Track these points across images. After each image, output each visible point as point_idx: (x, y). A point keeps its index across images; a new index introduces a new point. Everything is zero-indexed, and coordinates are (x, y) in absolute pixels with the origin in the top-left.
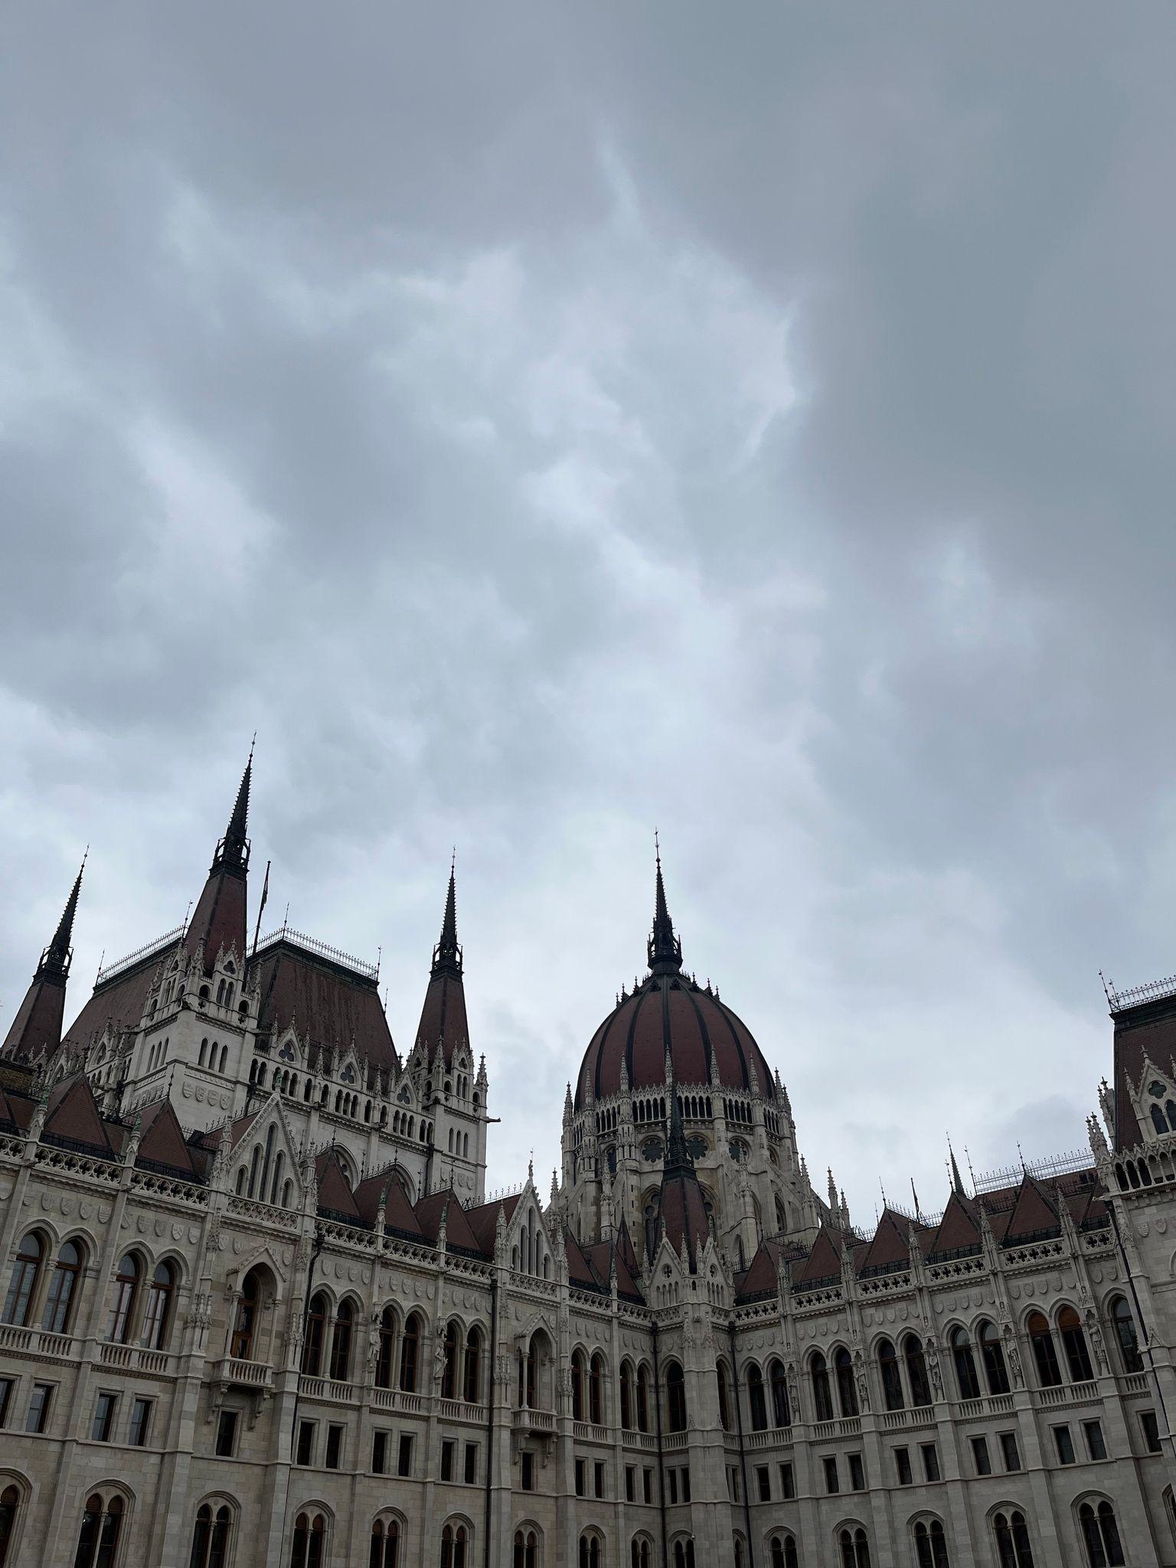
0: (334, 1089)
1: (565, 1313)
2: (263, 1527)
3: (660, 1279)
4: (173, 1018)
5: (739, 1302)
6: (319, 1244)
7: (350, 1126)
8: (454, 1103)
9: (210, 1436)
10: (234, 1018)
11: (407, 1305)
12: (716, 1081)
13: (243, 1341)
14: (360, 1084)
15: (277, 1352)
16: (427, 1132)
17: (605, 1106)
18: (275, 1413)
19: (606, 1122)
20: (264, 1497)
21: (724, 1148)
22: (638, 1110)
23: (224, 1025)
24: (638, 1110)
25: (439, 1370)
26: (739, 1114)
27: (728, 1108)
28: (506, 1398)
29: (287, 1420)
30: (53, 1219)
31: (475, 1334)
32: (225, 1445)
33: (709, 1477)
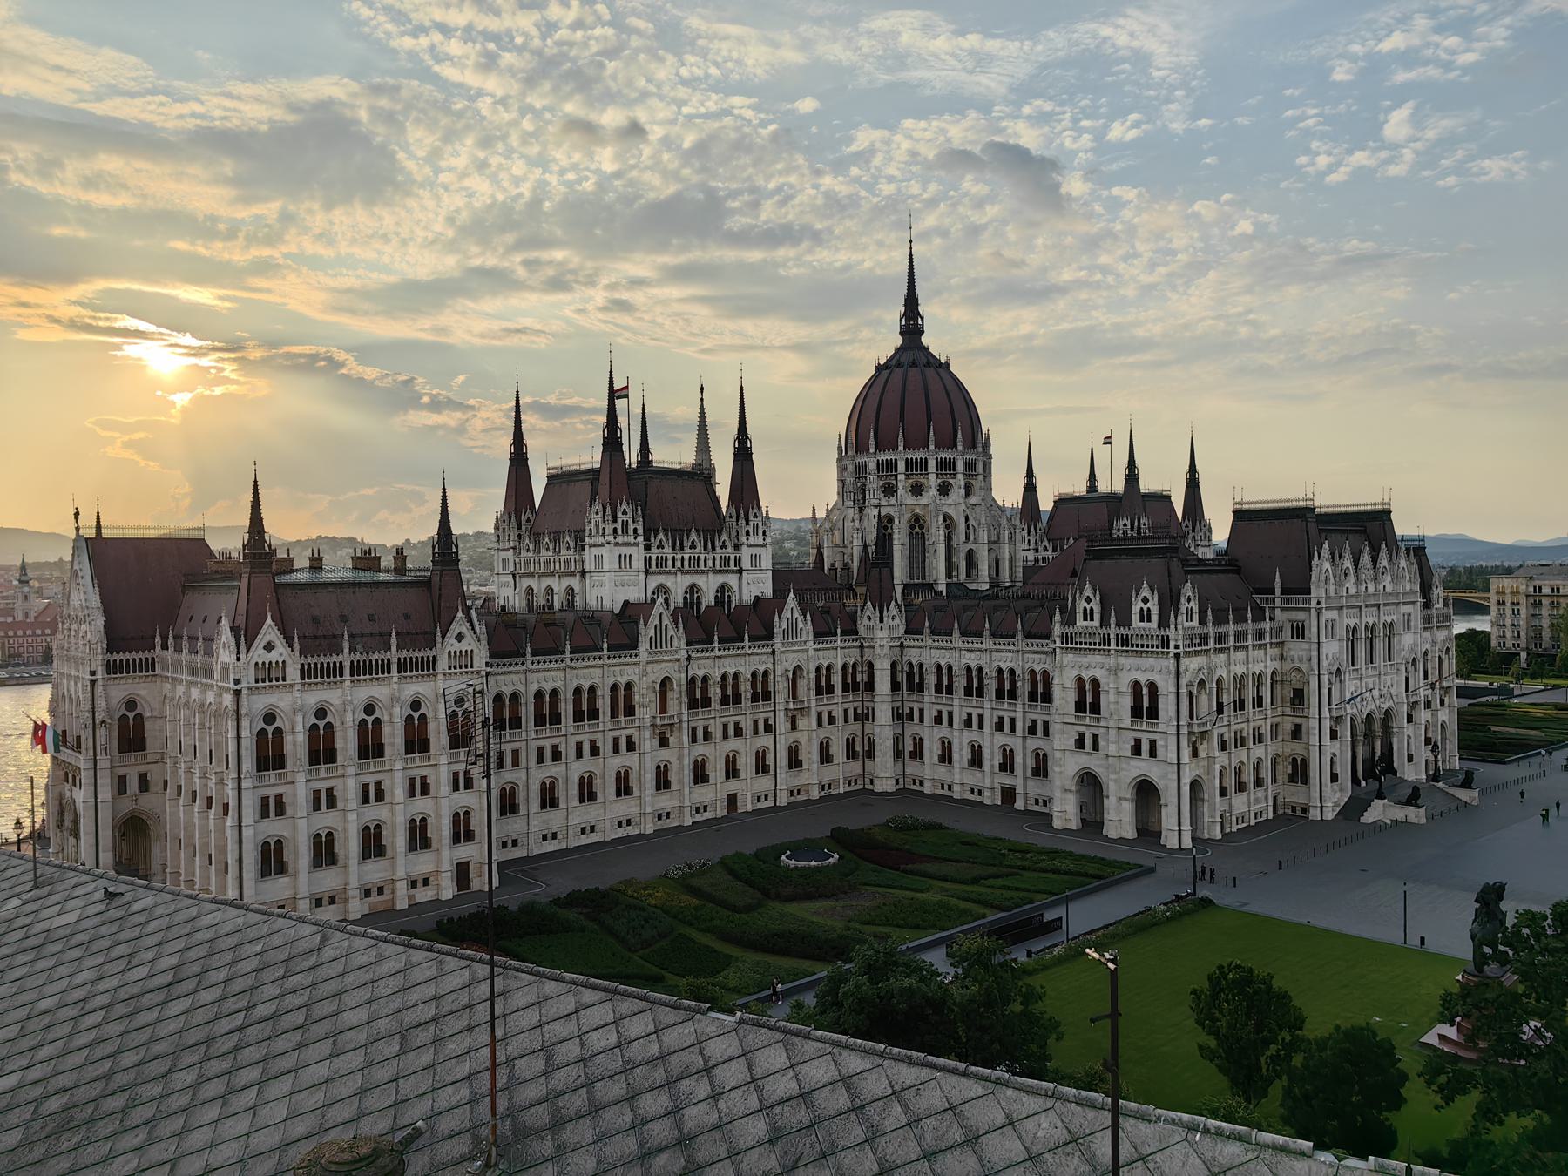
0: (686, 557)
1: (811, 652)
2: (681, 768)
3: (866, 621)
4: (602, 545)
5: (906, 632)
6: (689, 658)
7: (697, 572)
8: (752, 541)
9: (656, 742)
10: (631, 539)
11: (732, 671)
12: (932, 447)
13: (663, 709)
14: (700, 548)
15: (677, 704)
16: (738, 561)
17: (862, 459)
18: (680, 729)
19: (861, 469)
20: (680, 758)
21: (934, 492)
22: (881, 466)
23: (628, 544)
24: (881, 466)
25: (749, 695)
26: (946, 467)
27: (940, 464)
28: (780, 699)
29: (685, 732)
30: (582, 682)
31: (766, 673)
32: (664, 743)
33: (883, 714)
